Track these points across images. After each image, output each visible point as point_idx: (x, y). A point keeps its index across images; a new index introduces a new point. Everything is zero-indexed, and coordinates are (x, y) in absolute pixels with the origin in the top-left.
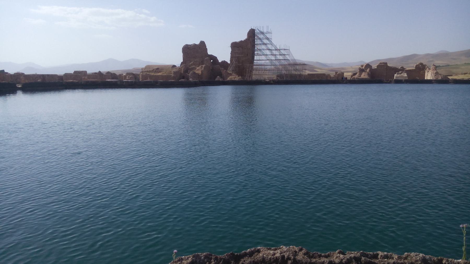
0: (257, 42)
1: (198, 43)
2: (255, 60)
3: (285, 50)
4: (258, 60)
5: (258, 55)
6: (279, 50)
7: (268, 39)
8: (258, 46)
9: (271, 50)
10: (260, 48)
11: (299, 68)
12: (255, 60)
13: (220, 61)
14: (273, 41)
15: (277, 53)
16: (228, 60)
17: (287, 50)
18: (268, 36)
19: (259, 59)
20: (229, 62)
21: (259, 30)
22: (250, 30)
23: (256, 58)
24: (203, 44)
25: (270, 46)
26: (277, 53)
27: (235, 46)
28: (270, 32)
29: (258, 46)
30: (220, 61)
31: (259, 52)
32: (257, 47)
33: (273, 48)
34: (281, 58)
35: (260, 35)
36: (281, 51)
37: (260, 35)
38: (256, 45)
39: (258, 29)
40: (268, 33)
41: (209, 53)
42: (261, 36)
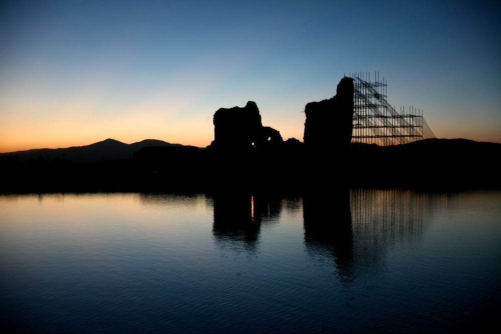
0: (358, 102)
1: (242, 105)
2: (354, 137)
3: (412, 116)
4: (358, 137)
5: (359, 127)
6: (401, 117)
7: (377, 96)
8: (360, 110)
9: (384, 117)
10: (362, 113)
11: (364, 90)
12: (354, 137)
13: (285, 139)
14: (390, 101)
15: (396, 122)
16: (300, 135)
17: (415, 116)
18: (380, 90)
19: (361, 134)
20: (302, 140)
21: (361, 81)
22: (343, 80)
23: (355, 132)
24: (252, 107)
25: (381, 110)
26: (396, 122)
27: (311, 109)
28: (382, 83)
29: (360, 110)
30: (285, 139)
31: (362, 123)
32: (358, 112)
33: (389, 114)
34: (405, 132)
35: (362, 90)
36: (405, 119)
37: (362, 90)
38: (356, 108)
39: (358, 78)
40: (377, 84)
41: (265, 123)
42: (363, 91)
